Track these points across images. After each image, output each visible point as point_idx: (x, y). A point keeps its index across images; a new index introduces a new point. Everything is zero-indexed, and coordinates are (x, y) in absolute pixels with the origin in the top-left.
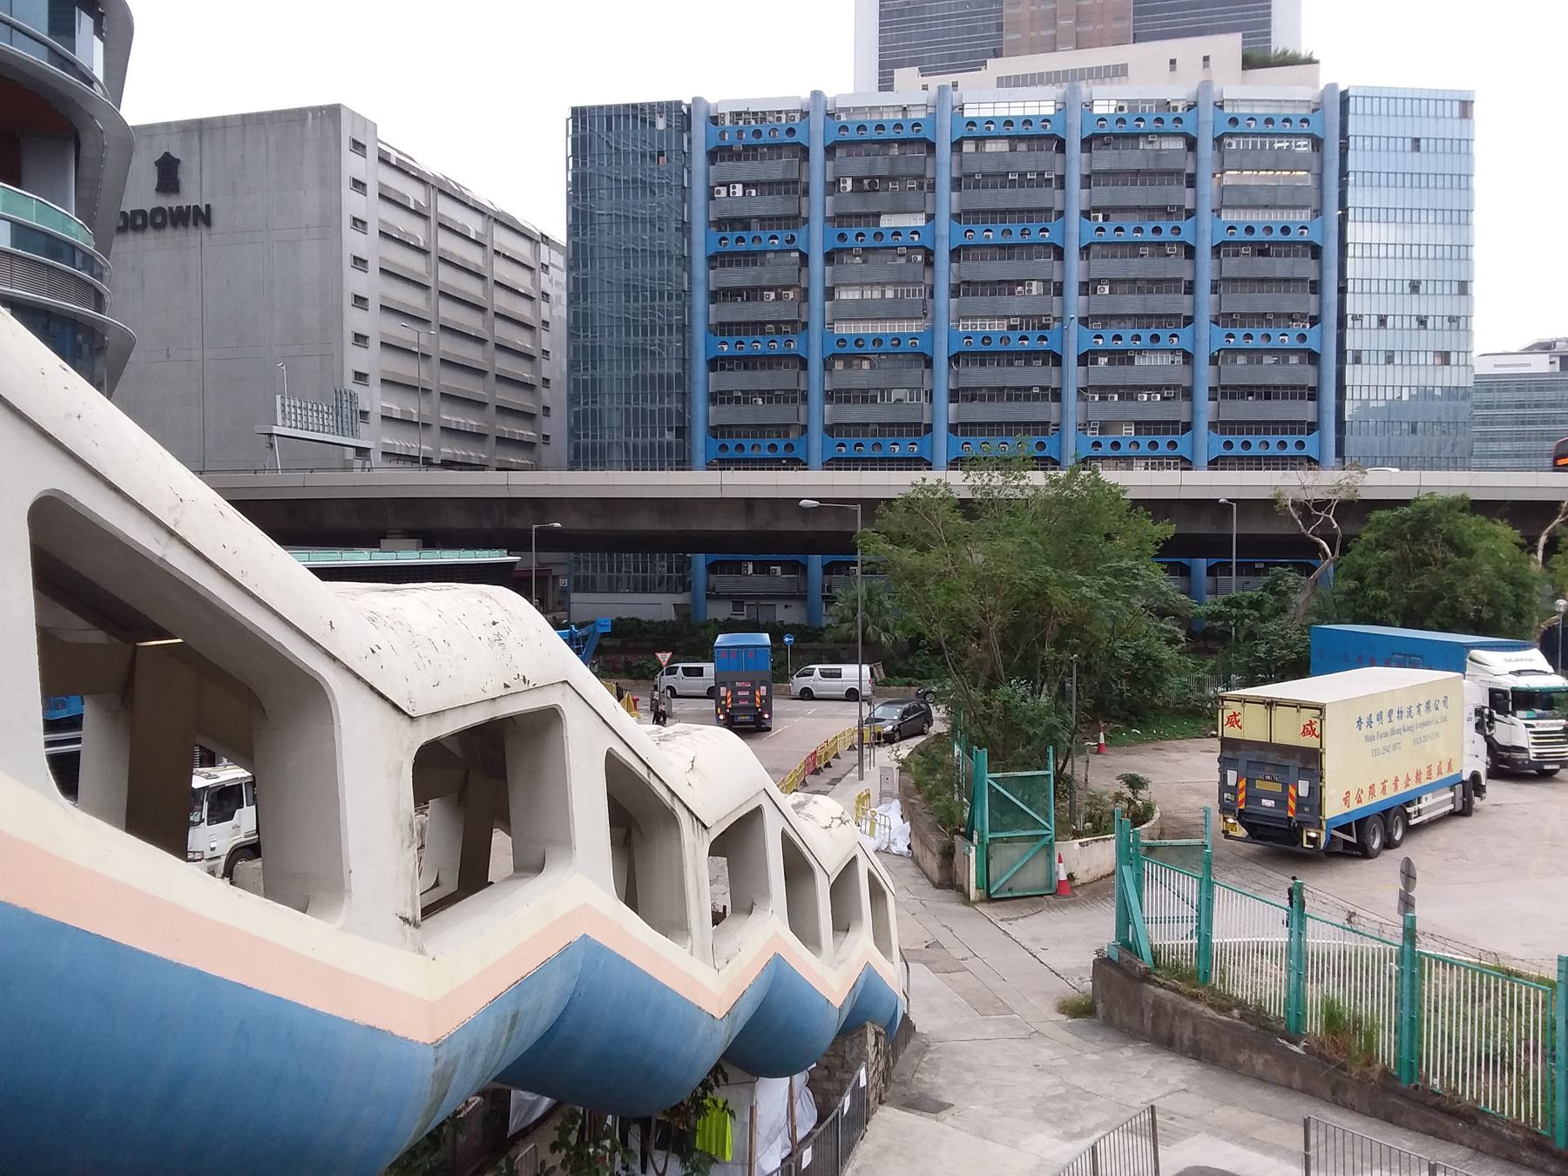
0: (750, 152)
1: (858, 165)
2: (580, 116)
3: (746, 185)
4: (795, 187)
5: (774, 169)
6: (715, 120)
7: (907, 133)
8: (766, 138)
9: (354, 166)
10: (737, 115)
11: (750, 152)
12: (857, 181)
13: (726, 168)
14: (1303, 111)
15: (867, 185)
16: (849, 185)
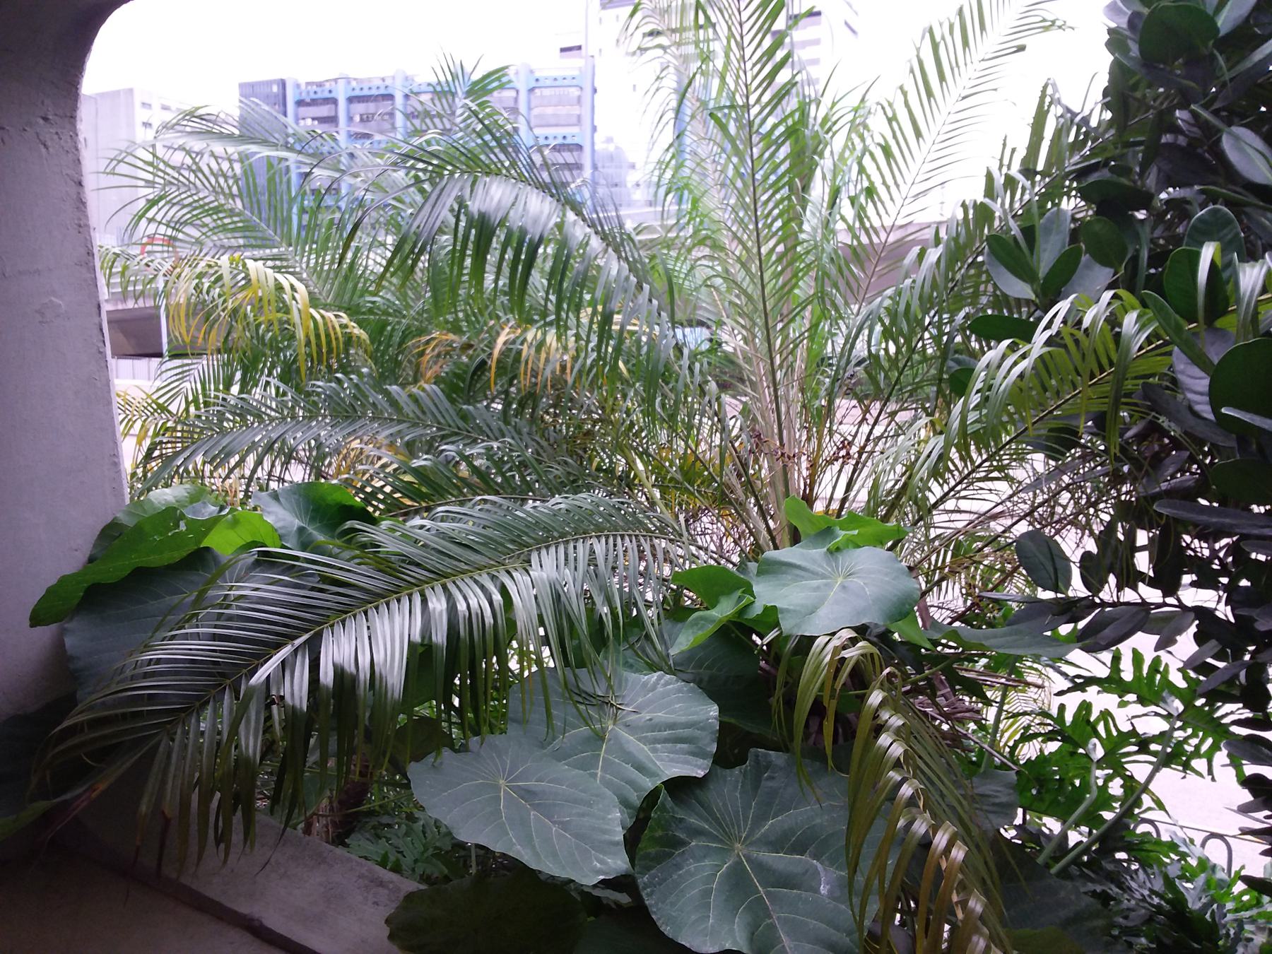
0: (314, 102)
1: (360, 108)
2: (242, 86)
3: (313, 119)
4: (332, 120)
5: (324, 111)
6: (298, 86)
7: (382, 91)
8: (319, 96)
9: (141, 115)
10: (308, 84)
11: (314, 102)
12: (361, 115)
13: (303, 111)
14: (576, 73)
15: (365, 119)
16: (357, 118)
